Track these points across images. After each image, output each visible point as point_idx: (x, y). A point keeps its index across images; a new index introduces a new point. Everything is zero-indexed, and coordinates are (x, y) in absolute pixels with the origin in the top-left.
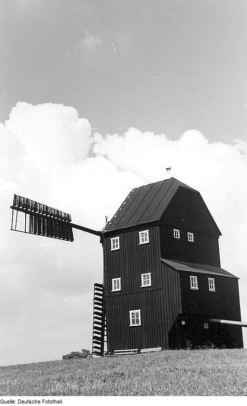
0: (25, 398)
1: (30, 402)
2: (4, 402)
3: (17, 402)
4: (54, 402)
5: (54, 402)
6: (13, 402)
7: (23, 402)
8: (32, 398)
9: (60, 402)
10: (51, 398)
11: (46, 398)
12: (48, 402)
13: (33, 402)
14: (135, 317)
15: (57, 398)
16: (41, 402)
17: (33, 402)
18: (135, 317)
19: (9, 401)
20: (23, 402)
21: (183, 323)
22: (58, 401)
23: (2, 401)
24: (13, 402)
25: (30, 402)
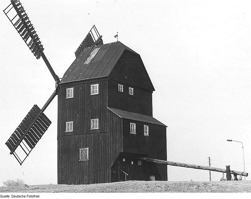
0: (16, 194)
1: (19, 197)
3: (11, 196)
4: (34, 196)
6: (8, 196)
8: (20, 194)
11: (30, 194)
13: (21, 196)
14: (85, 153)
17: (21, 196)
18: (85, 153)
19: (5, 196)
20: (14, 196)
21: (124, 160)
22: (37, 196)
23: (1, 196)
25: (19, 197)
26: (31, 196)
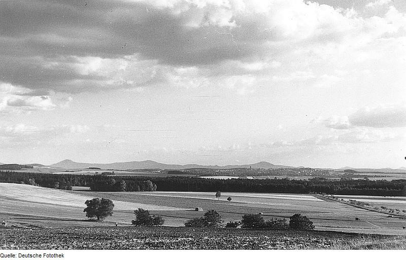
1: (31, 256)
2: (4, 256)
3: (17, 256)
4: (55, 255)
5: (55, 255)
6: (13, 256)
7: (23, 256)
9: (61, 256)
10: (53, 252)
11: (48, 252)
12: (50, 256)
13: (34, 256)
15: (59, 252)
16: (42, 256)
17: (34, 256)
19: (9, 255)
20: (23, 256)
22: (60, 255)
23: (2, 255)
24: (13, 256)
25: (31, 256)
26: (50, 256)
